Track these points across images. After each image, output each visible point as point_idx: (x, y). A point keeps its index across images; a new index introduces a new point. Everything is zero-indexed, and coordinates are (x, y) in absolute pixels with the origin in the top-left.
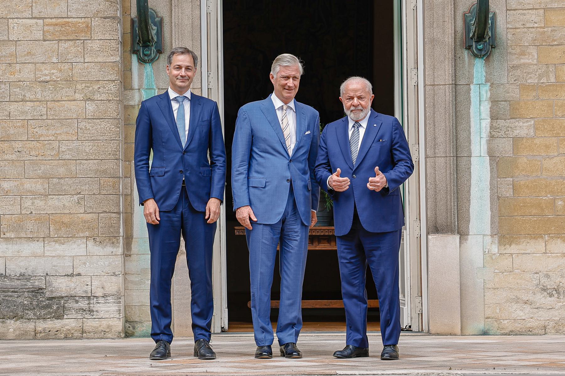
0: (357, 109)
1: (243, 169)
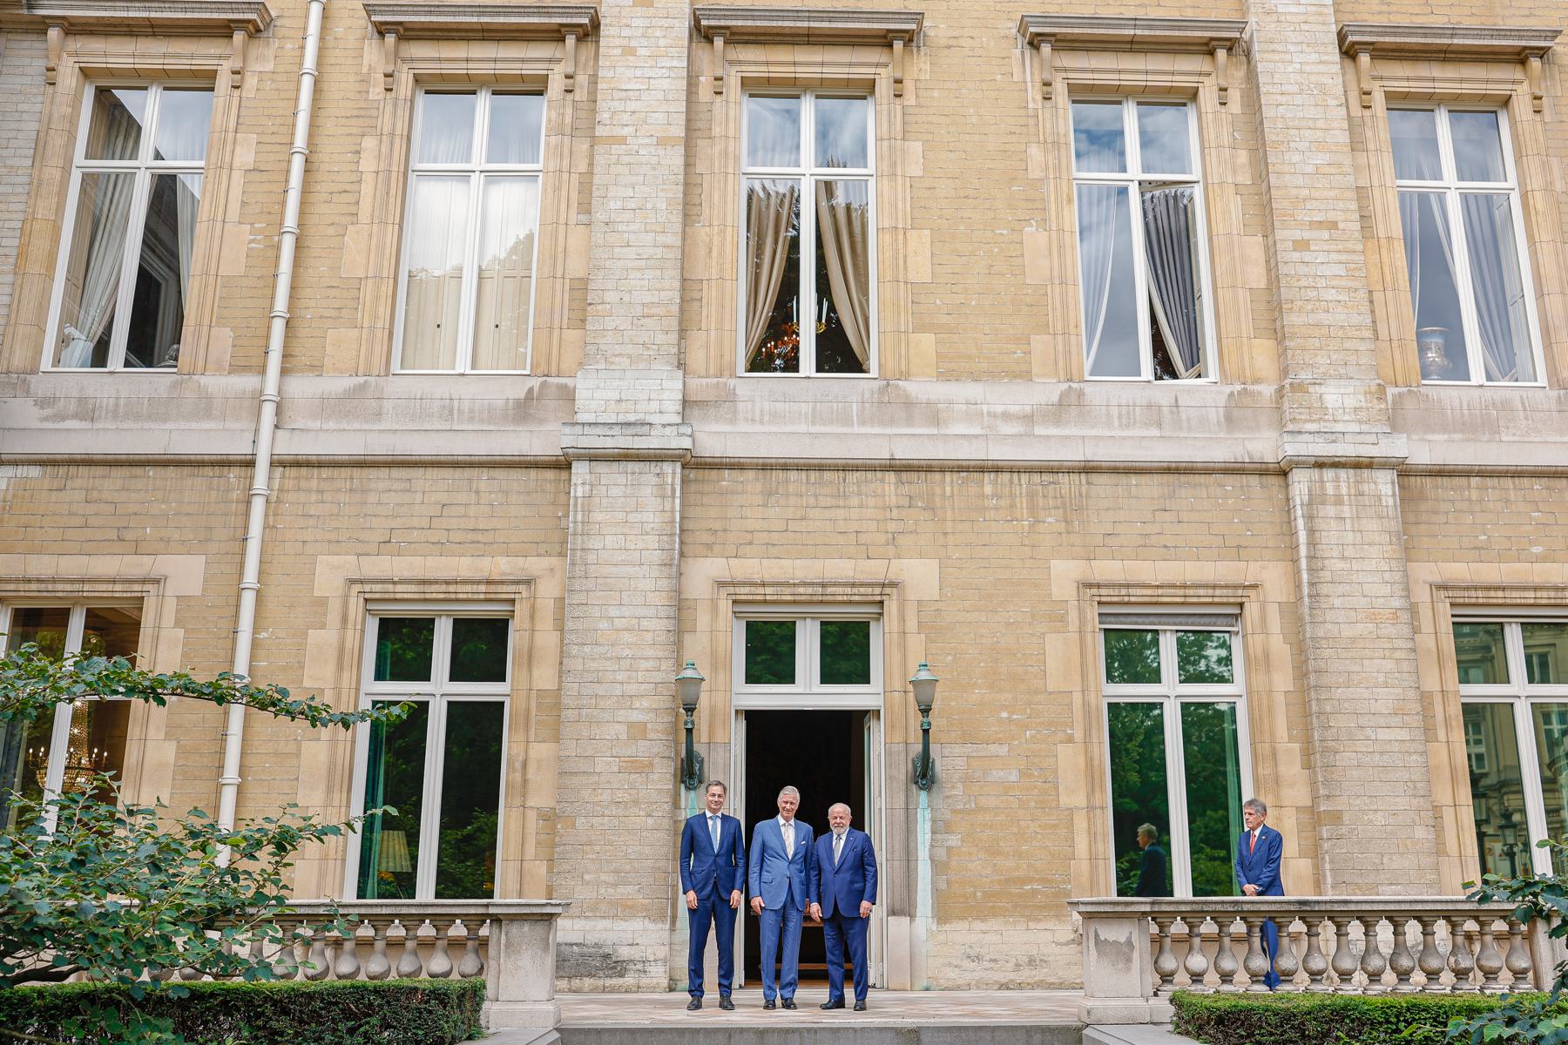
0: (839, 825)
1: (757, 869)
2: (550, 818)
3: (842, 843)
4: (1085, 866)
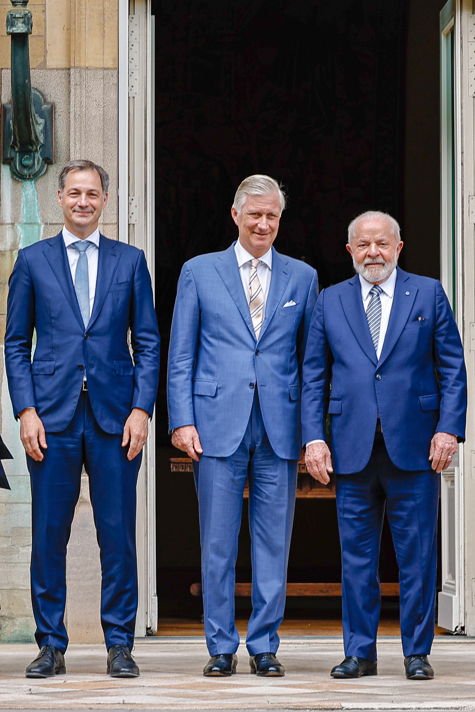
0: (374, 261)
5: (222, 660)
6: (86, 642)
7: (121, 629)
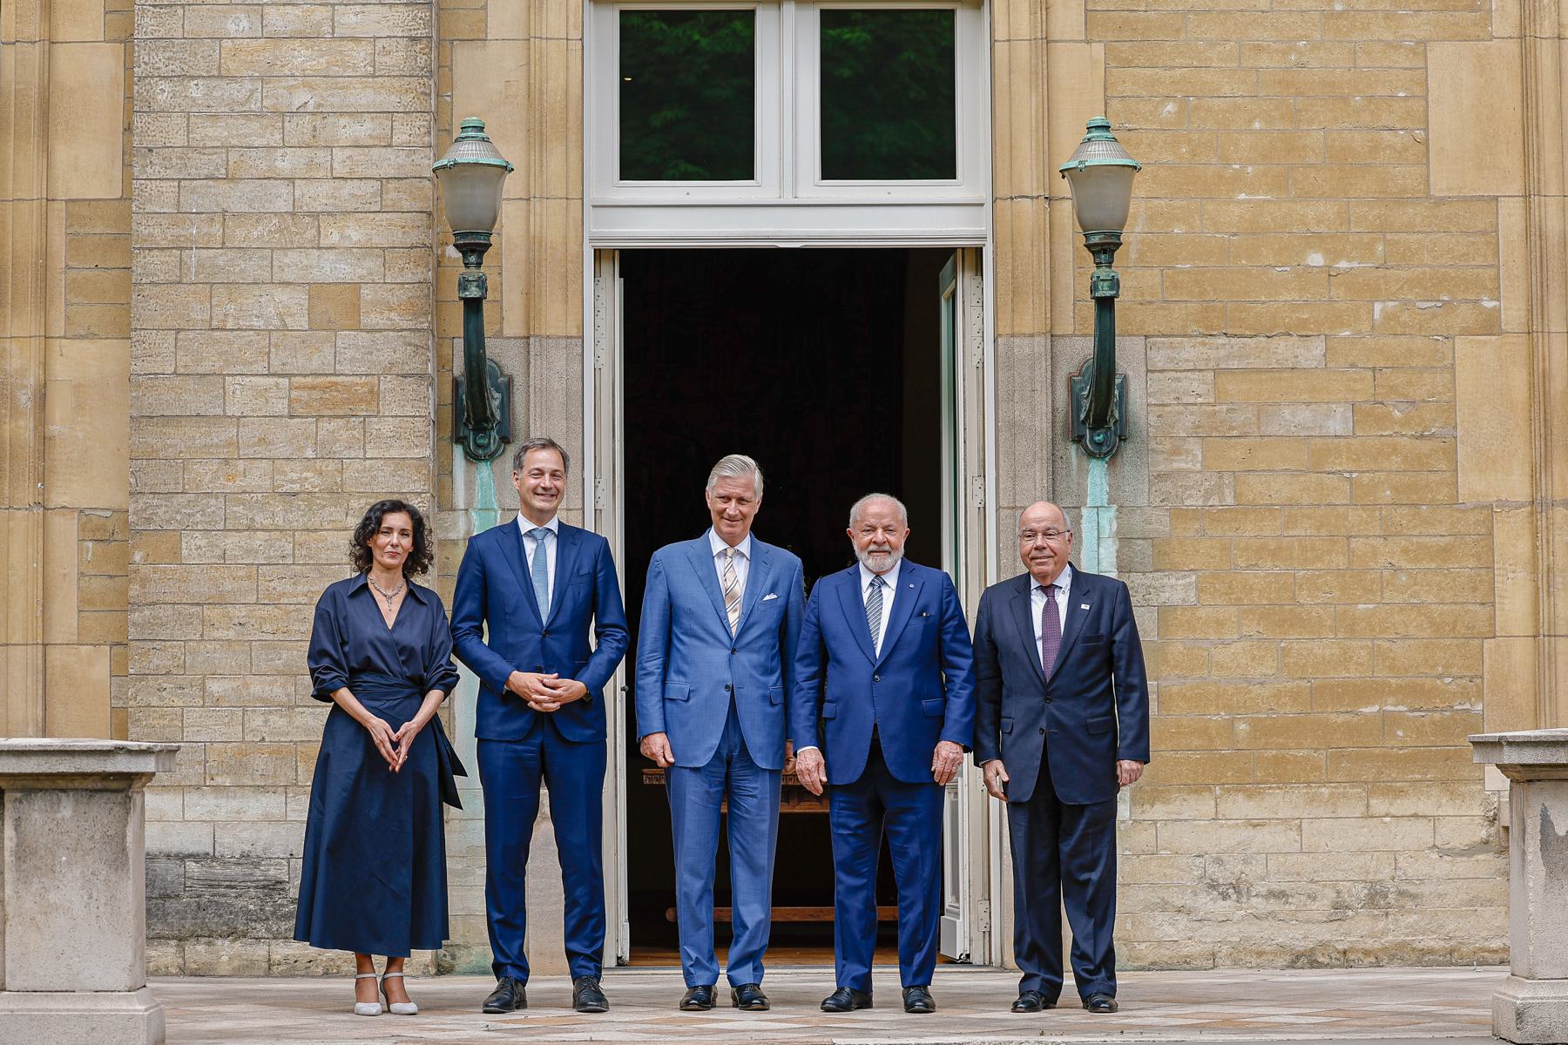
2: (113, 536)
3: (889, 595)
4: (1521, 654)
5: (700, 992)
6: (549, 974)
7: (588, 958)
